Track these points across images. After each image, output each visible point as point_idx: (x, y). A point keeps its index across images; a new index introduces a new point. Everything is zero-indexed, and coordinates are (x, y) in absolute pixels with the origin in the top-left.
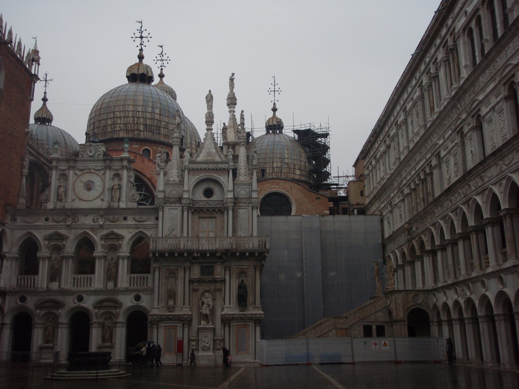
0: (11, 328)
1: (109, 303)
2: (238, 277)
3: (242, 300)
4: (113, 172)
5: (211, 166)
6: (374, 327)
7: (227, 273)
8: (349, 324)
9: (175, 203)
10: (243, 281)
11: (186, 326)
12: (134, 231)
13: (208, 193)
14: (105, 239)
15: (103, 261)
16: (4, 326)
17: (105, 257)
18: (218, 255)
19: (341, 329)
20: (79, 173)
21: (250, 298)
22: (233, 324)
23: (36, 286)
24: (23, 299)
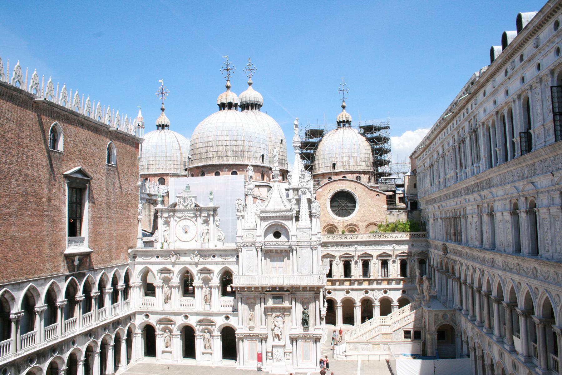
1: (206, 322)
3: (305, 322)
4: (202, 218)
5: (278, 214)
9: (251, 246)
11: (264, 342)
13: (277, 235)
20: (178, 220)
21: (311, 321)
22: (299, 342)
24: (147, 316)
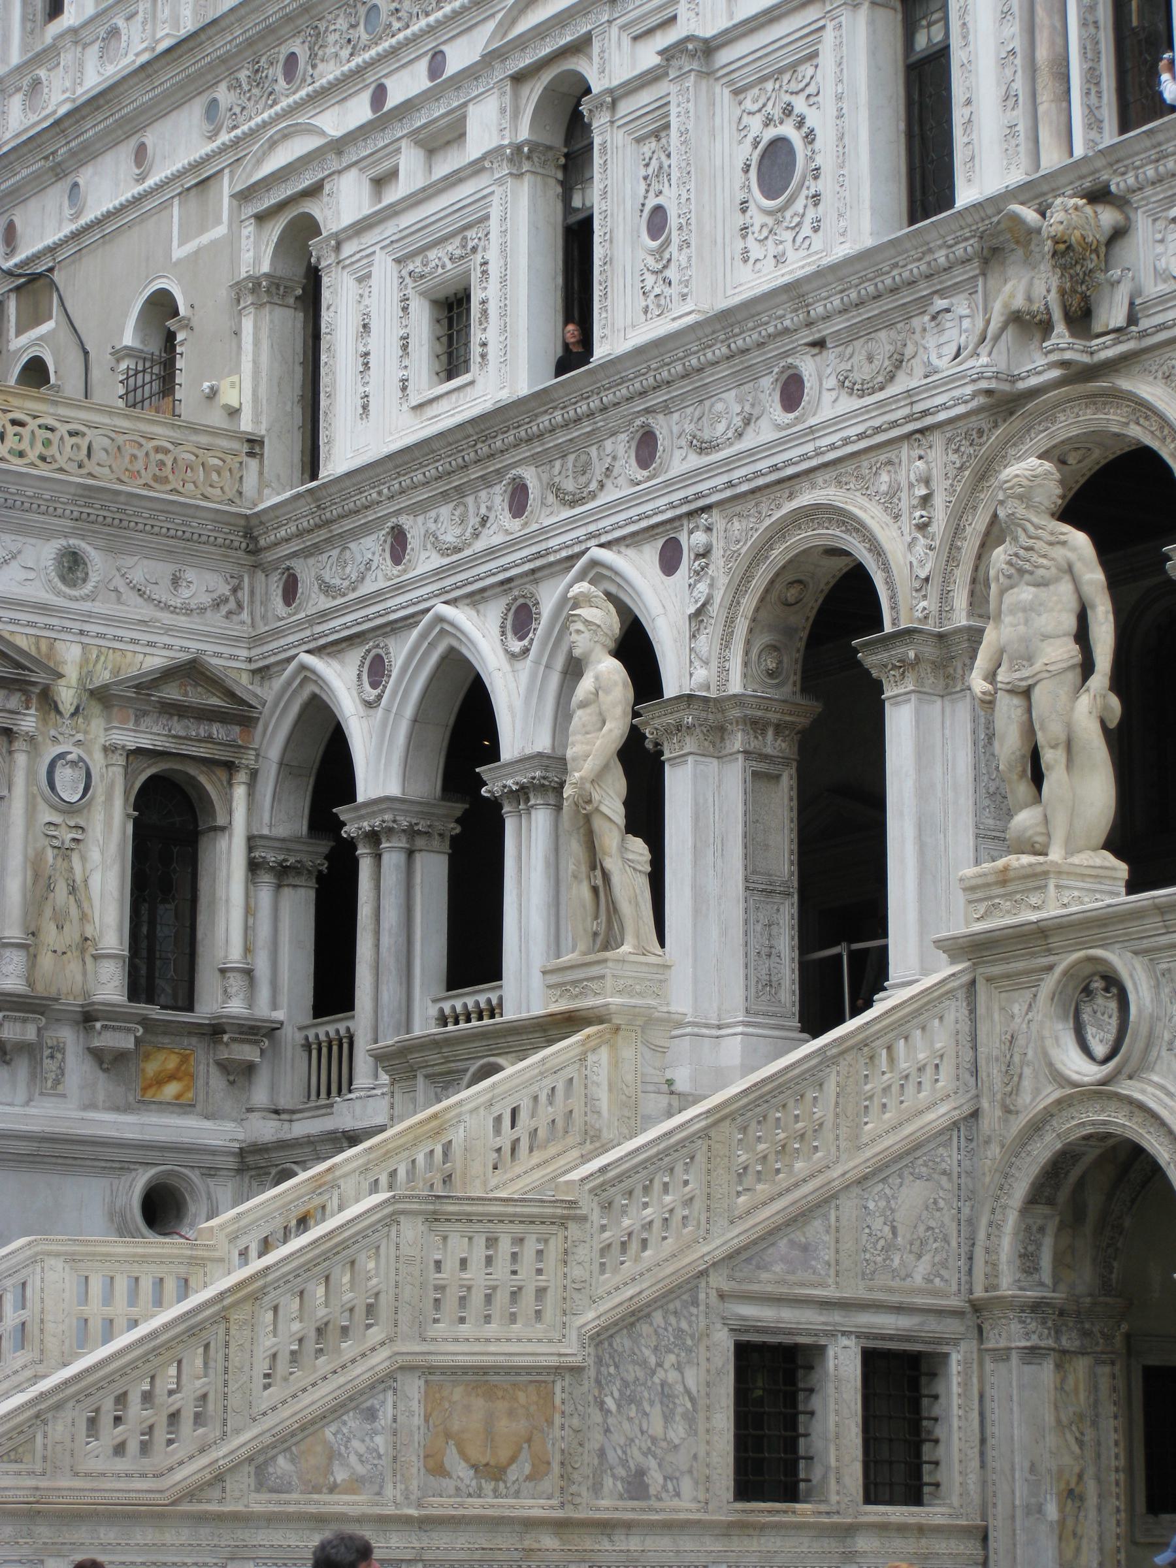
6: (843, 1368)
8: (589, 1317)
19: (482, 1378)
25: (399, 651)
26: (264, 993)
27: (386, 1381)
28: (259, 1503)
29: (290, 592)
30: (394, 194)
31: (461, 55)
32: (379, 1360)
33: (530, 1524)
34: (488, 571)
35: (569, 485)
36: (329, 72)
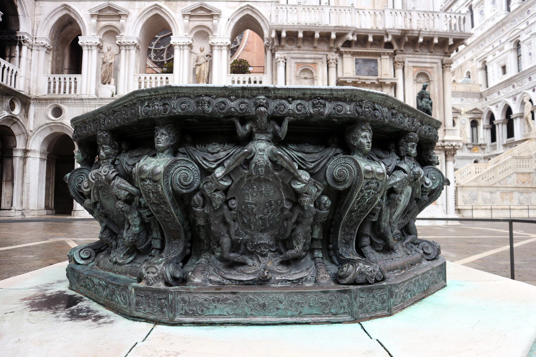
0: (41, 159)
2: (416, 81)
7: (399, 72)
10: (424, 88)
12: (238, 5)
14: (191, 16)
15: (186, 52)
16: (29, 154)
17: (190, 46)
18: (390, 39)
19: (523, 173)
23: (78, 92)
24: (58, 112)
25: (499, 105)
26: (485, 141)
27: (512, 174)
28: (500, 186)
29: (486, 100)
30: (495, 57)
31: (503, 40)
32: (511, 172)
33: (528, 188)
34: (511, 95)
35: (520, 84)
36: (487, 45)
